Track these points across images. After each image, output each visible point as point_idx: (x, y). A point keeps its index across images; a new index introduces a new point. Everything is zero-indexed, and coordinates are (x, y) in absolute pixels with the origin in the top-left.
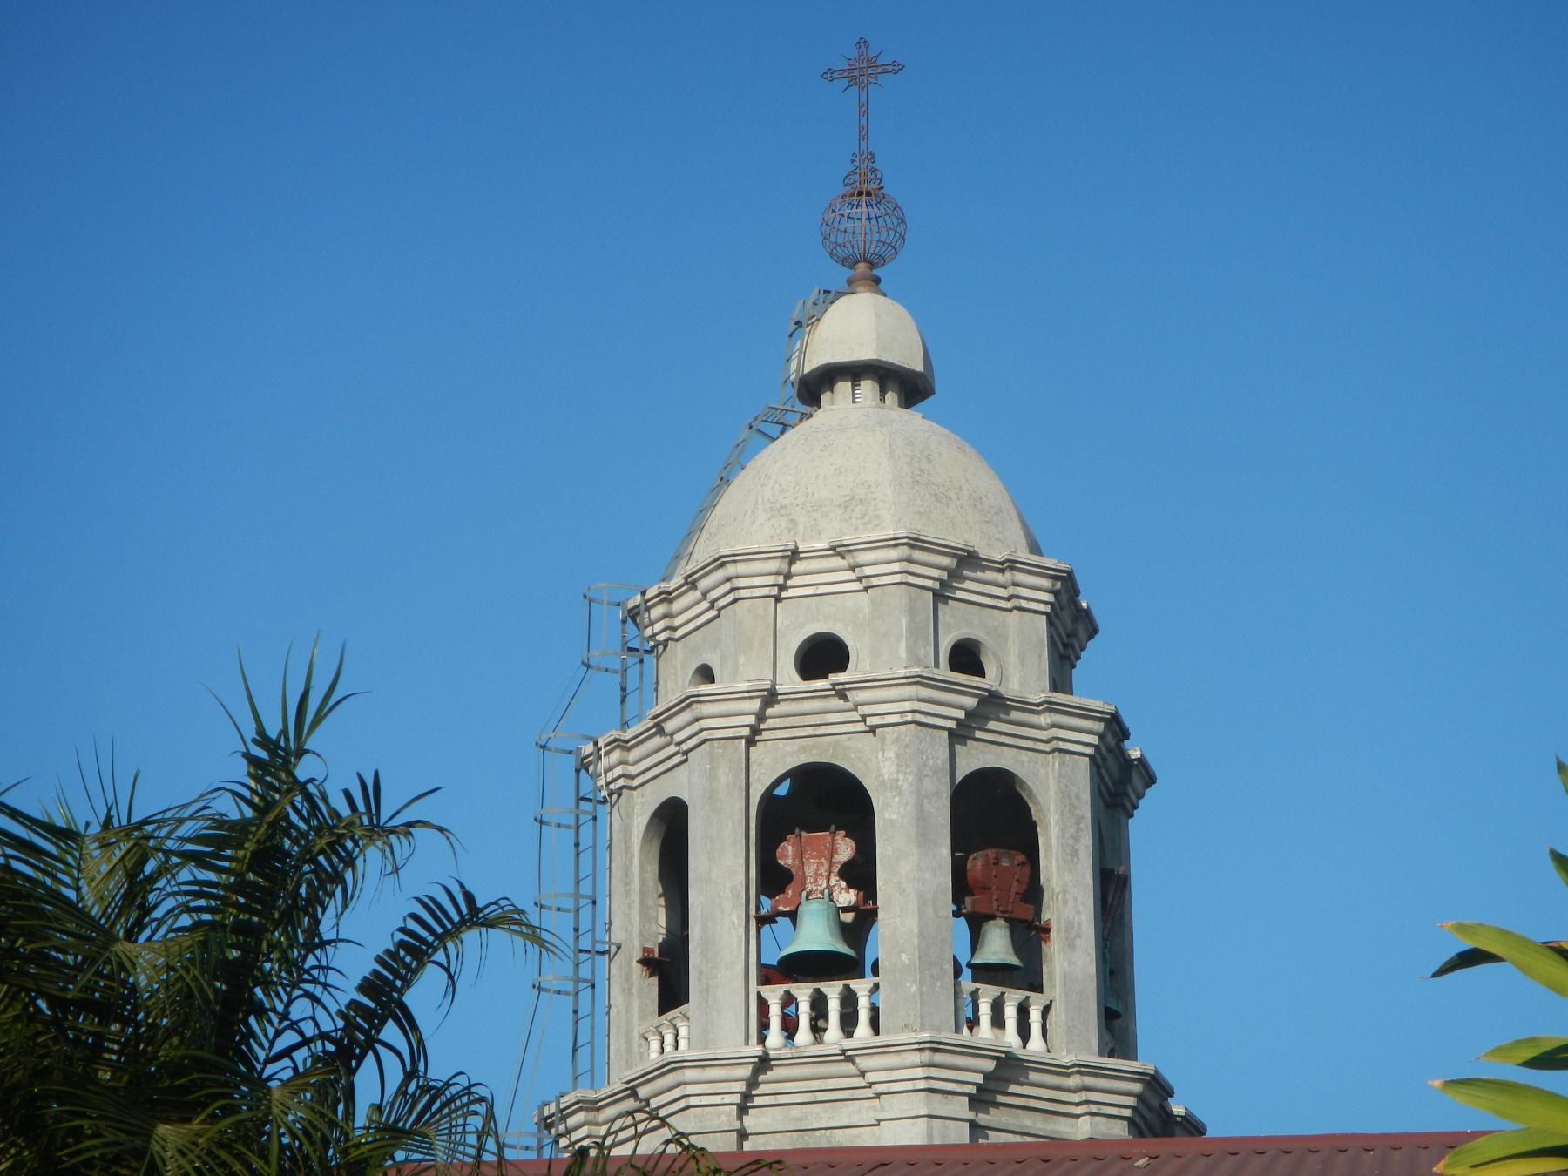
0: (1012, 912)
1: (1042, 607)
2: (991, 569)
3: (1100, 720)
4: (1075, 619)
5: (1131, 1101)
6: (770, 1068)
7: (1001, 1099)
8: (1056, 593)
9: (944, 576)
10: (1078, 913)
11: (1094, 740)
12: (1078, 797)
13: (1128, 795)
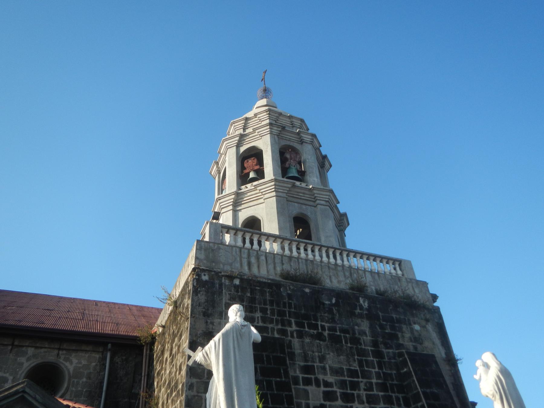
1: (267, 118)
2: (254, 118)
3: (268, 125)
4: (290, 119)
5: (273, 187)
7: (243, 202)
8: (269, 114)
9: (243, 124)
11: (269, 130)
12: (267, 142)
13: (304, 139)
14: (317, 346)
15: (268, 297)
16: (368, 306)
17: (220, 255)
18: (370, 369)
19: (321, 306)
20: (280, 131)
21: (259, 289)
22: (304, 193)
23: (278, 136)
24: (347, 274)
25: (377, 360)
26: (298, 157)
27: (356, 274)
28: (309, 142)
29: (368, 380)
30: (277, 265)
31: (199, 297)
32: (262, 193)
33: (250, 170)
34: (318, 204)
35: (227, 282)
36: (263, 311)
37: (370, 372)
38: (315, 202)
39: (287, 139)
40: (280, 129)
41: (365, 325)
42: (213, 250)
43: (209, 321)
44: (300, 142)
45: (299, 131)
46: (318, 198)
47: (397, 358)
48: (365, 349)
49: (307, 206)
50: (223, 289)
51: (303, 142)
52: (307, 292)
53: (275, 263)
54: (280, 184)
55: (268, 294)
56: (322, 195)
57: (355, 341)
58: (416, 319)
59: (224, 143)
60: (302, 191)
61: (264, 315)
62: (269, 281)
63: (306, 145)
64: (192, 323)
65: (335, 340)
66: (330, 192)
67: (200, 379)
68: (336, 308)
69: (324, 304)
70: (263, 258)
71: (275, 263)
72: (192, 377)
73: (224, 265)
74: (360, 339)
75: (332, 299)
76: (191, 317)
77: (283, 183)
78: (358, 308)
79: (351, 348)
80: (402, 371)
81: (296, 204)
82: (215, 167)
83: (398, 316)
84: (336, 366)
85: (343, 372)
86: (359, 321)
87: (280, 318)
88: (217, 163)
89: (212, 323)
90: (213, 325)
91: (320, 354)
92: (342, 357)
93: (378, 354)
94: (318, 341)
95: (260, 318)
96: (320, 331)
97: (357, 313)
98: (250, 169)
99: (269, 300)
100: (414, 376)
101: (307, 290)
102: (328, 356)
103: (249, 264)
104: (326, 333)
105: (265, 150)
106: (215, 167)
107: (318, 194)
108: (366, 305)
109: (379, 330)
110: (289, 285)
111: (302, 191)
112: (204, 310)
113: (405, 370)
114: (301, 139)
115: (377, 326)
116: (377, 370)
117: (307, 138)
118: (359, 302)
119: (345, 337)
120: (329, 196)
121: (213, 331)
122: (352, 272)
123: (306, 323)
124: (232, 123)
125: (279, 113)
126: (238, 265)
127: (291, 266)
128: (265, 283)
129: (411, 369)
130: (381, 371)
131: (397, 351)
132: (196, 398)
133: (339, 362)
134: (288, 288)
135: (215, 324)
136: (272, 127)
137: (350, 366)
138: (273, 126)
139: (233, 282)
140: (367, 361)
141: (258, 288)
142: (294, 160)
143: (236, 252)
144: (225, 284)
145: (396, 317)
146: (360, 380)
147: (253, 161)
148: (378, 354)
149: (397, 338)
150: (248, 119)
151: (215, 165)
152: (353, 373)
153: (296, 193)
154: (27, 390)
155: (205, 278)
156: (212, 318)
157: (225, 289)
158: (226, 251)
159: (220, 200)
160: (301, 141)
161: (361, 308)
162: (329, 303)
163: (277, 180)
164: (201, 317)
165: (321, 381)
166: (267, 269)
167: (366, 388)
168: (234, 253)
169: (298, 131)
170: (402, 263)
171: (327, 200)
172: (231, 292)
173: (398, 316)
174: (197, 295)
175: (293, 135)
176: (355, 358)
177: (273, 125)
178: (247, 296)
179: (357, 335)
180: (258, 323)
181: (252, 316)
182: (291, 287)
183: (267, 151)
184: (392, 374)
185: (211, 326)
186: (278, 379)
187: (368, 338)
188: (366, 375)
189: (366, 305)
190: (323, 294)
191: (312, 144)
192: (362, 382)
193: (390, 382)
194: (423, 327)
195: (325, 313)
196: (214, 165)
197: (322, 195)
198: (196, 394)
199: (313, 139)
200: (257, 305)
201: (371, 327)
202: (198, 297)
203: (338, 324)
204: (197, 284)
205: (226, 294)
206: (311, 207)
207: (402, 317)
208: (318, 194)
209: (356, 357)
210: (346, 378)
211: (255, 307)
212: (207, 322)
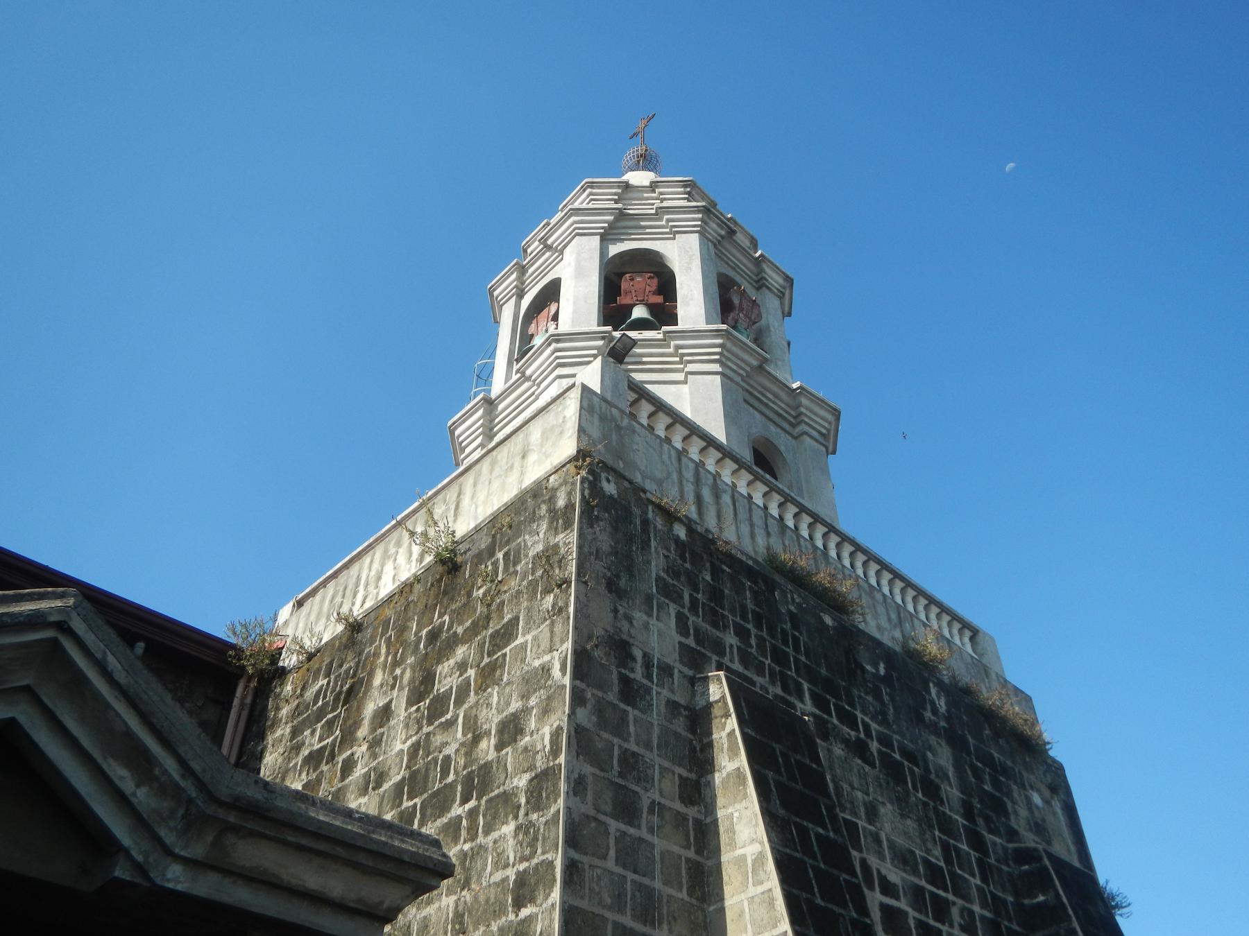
0: (647, 301)
3: (698, 212)
6: (497, 406)
8: (689, 193)
10: (691, 291)
12: (690, 248)
13: (767, 280)
14: (859, 771)
15: (749, 601)
16: (947, 711)
17: (635, 447)
18: (967, 876)
19: (859, 672)
20: (722, 237)
21: (728, 573)
22: (776, 396)
23: (715, 245)
24: (894, 616)
25: (977, 855)
26: (756, 311)
27: (909, 624)
28: (776, 291)
29: (967, 905)
30: (757, 531)
31: (598, 533)
32: (683, 355)
33: (637, 300)
34: (806, 433)
35: (659, 522)
36: (742, 633)
37: (966, 880)
38: (793, 426)
39: (730, 263)
40: (723, 233)
41: (943, 757)
42: (619, 428)
43: (621, 610)
44: (755, 284)
45: (761, 255)
46: (806, 420)
47: (1011, 863)
48: (950, 817)
49: (779, 430)
50: (652, 535)
51: (764, 285)
52: (828, 626)
53: (752, 525)
54: (734, 349)
55: (748, 592)
56: (816, 414)
57: (931, 790)
58: (1032, 778)
59: (569, 217)
60: (775, 389)
61: (743, 646)
62: (750, 563)
63: (769, 295)
64: (581, 598)
65: (893, 772)
66: (833, 414)
67: (602, 770)
68: (888, 690)
69: (863, 669)
70: (726, 498)
71: (752, 525)
72: (581, 757)
73: (644, 477)
74: (938, 788)
75: (879, 665)
76: (577, 580)
77: (742, 348)
78: (929, 707)
79: (925, 805)
80: (1027, 902)
81: (757, 415)
82: (514, 276)
83: (1001, 758)
84: (900, 841)
85: (916, 864)
86: (933, 740)
87: (778, 668)
88: (522, 270)
89: (630, 619)
90: (631, 623)
91: (866, 797)
92: (909, 822)
93: (977, 842)
94: (859, 762)
95: (735, 650)
96: (862, 736)
97: (927, 719)
98: (635, 298)
99: (753, 612)
100: (1074, 919)
101: (828, 620)
102: (882, 810)
103: (699, 500)
104: (874, 746)
105: (685, 265)
106: (514, 276)
107: (807, 408)
108: (942, 705)
109: (973, 780)
110: (790, 590)
111: (775, 389)
112: (609, 574)
113: (1041, 898)
114: (760, 276)
115: (967, 768)
116: (978, 882)
117: (775, 280)
118: (930, 693)
119: (912, 773)
120: (830, 423)
121: (631, 641)
122: (902, 615)
123: (832, 703)
124: (587, 183)
125: (712, 201)
126: (674, 492)
127: (784, 544)
128: (740, 561)
129: (1065, 900)
130: (985, 887)
131: (1011, 845)
132: (593, 824)
133: (905, 833)
134: (789, 596)
135: (635, 622)
136: (708, 221)
137: (928, 851)
138: (710, 219)
139: (673, 530)
140: (957, 850)
141: (728, 570)
142: (746, 316)
143: (670, 457)
144: (655, 527)
145: (999, 758)
146: (951, 897)
147: (649, 281)
148: (977, 842)
149: (1007, 815)
150: (629, 189)
151: (515, 273)
152: (935, 875)
153: (760, 389)
154: (78, 626)
155: (610, 488)
156: (628, 603)
157: (655, 539)
158: (647, 442)
159: (558, 341)
160: (757, 282)
161: (935, 711)
162: (874, 671)
163: (731, 337)
164: (602, 589)
165: (875, 873)
166: (737, 531)
167: (962, 922)
168: (665, 457)
169: (757, 255)
170: (980, 637)
171: (824, 431)
172: (669, 554)
173: (1001, 758)
174: (591, 526)
175: (745, 261)
176: (934, 835)
177: (712, 216)
178: (703, 579)
179: (933, 777)
180: (732, 661)
181: (718, 637)
182: (795, 596)
183: (690, 269)
184: (1006, 901)
185: (625, 625)
186: (821, 831)
187: (951, 791)
188: (960, 890)
189: (942, 705)
190: (860, 644)
191: (780, 298)
192: (954, 903)
193: (1006, 923)
194: (1047, 802)
195: (867, 693)
196: (512, 273)
197: (816, 414)
198: (592, 813)
199: (784, 288)
200: (726, 613)
201: (958, 766)
202: (595, 533)
203: (894, 732)
204: (590, 495)
205: (657, 553)
206: (787, 435)
207: (1009, 763)
208: (807, 408)
209: (937, 833)
210: (923, 883)
211: (724, 616)
212: (616, 611)
